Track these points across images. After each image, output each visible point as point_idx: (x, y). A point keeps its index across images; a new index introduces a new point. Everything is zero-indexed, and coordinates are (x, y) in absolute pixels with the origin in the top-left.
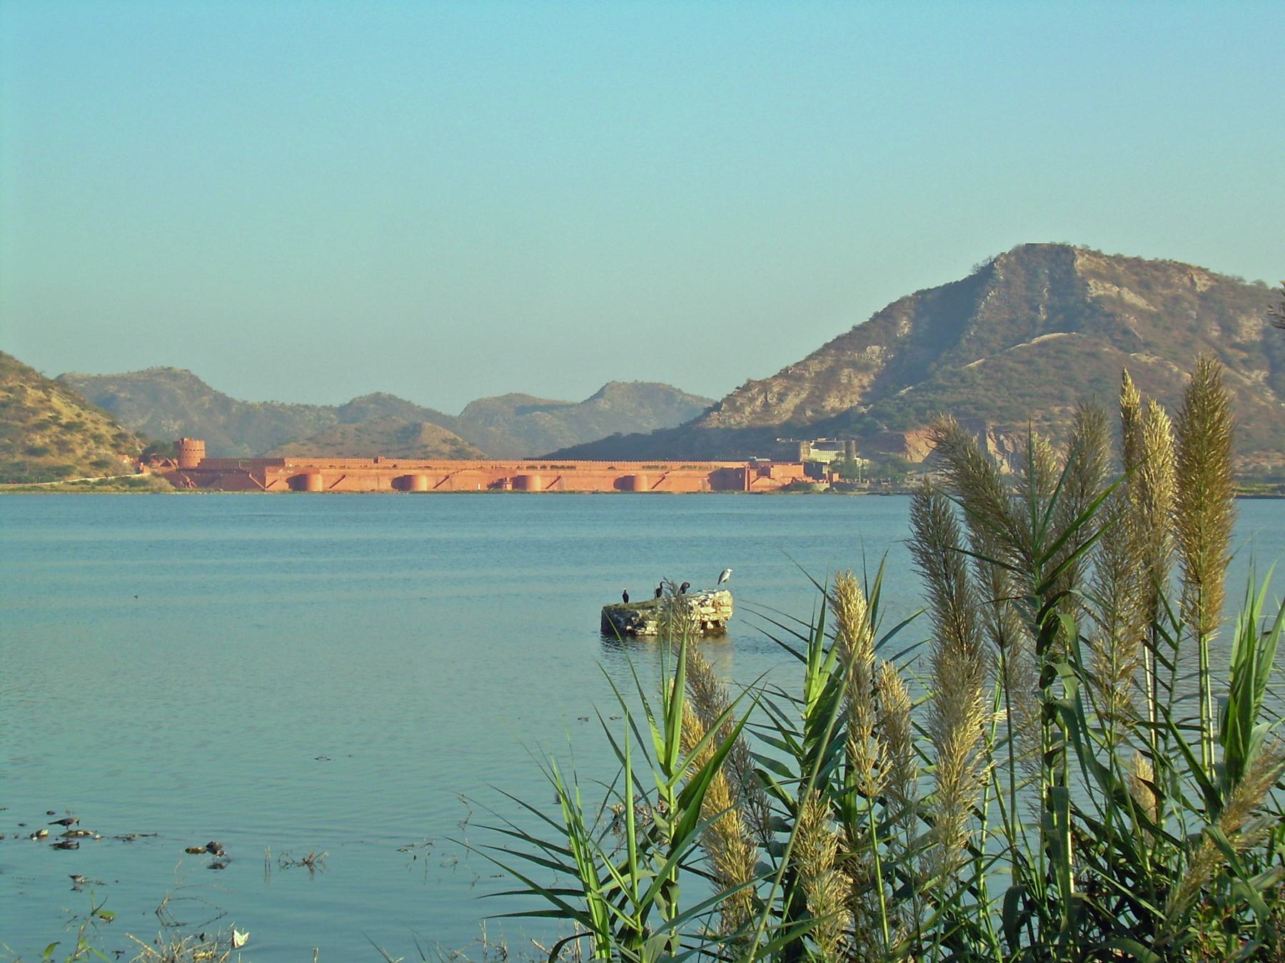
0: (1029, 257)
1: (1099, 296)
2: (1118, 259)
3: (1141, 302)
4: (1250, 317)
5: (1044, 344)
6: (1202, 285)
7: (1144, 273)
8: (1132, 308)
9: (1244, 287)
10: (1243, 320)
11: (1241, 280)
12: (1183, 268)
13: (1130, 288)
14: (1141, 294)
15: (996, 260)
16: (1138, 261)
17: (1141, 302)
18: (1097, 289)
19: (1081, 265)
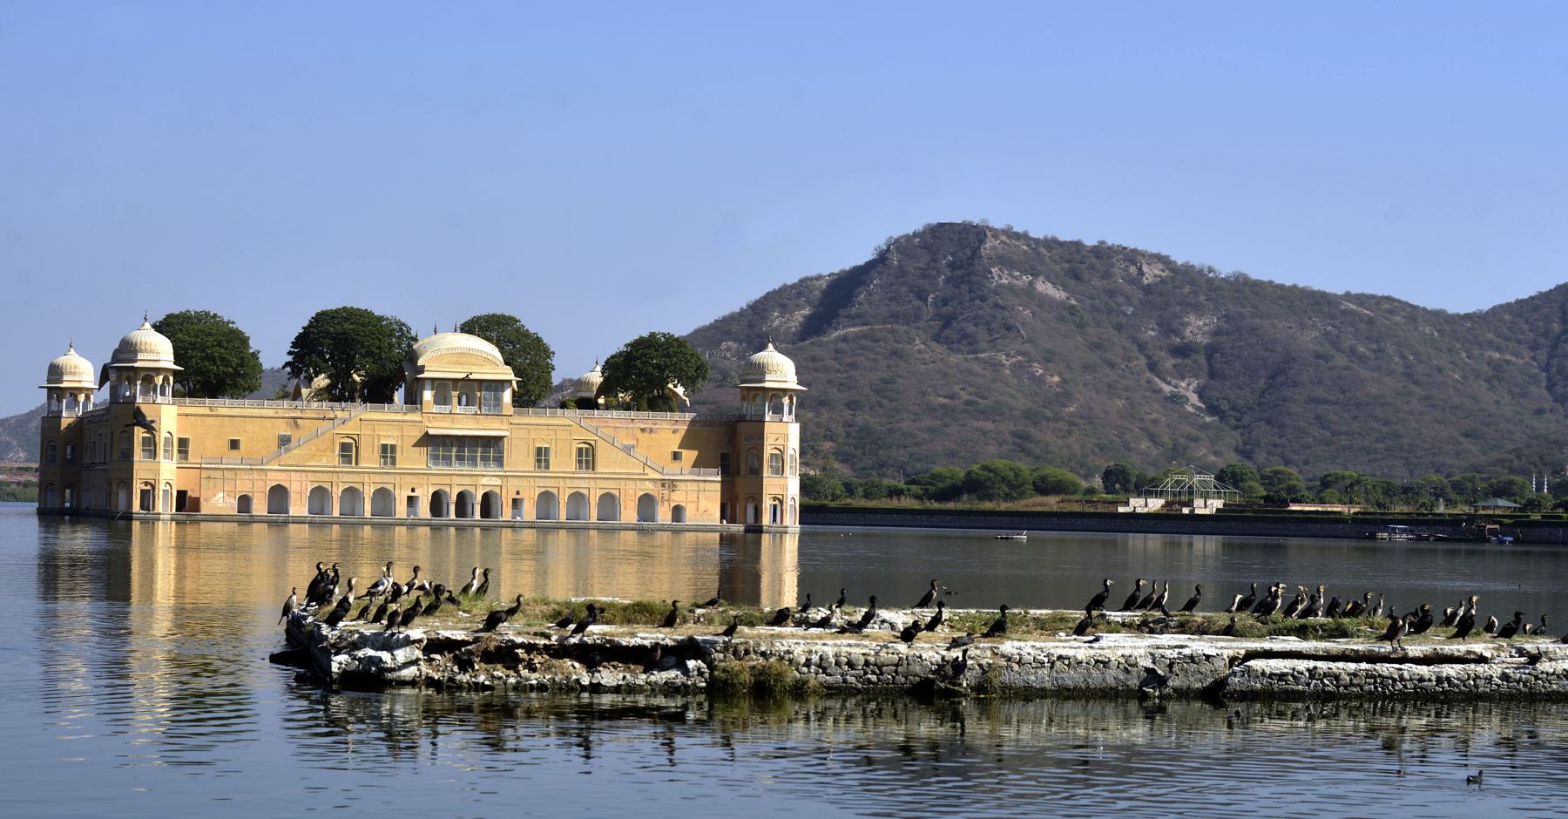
0: (938, 235)
1: (1002, 286)
2: (1051, 243)
3: (1059, 294)
4: (1200, 317)
5: (845, 339)
6: (1151, 273)
7: (1075, 262)
8: (1045, 302)
9: (1210, 281)
10: (1192, 318)
11: (1211, 270)
12: (1132, 256)
13: (1048, 279)
14: (1065, 288)
15: (897, 241)
16: (1077, 245)
17: (1059, 294)
18: (1001, 277)
19: (993, 248)
